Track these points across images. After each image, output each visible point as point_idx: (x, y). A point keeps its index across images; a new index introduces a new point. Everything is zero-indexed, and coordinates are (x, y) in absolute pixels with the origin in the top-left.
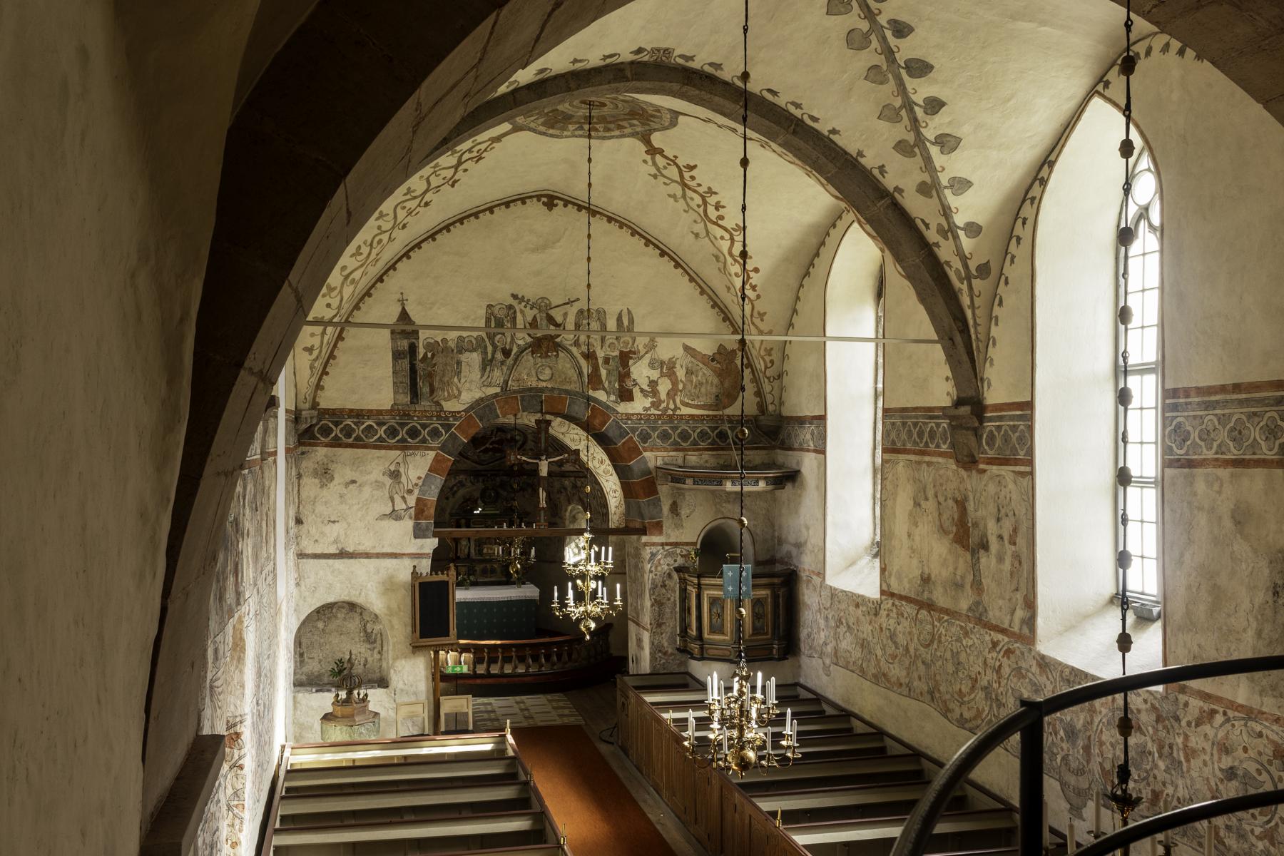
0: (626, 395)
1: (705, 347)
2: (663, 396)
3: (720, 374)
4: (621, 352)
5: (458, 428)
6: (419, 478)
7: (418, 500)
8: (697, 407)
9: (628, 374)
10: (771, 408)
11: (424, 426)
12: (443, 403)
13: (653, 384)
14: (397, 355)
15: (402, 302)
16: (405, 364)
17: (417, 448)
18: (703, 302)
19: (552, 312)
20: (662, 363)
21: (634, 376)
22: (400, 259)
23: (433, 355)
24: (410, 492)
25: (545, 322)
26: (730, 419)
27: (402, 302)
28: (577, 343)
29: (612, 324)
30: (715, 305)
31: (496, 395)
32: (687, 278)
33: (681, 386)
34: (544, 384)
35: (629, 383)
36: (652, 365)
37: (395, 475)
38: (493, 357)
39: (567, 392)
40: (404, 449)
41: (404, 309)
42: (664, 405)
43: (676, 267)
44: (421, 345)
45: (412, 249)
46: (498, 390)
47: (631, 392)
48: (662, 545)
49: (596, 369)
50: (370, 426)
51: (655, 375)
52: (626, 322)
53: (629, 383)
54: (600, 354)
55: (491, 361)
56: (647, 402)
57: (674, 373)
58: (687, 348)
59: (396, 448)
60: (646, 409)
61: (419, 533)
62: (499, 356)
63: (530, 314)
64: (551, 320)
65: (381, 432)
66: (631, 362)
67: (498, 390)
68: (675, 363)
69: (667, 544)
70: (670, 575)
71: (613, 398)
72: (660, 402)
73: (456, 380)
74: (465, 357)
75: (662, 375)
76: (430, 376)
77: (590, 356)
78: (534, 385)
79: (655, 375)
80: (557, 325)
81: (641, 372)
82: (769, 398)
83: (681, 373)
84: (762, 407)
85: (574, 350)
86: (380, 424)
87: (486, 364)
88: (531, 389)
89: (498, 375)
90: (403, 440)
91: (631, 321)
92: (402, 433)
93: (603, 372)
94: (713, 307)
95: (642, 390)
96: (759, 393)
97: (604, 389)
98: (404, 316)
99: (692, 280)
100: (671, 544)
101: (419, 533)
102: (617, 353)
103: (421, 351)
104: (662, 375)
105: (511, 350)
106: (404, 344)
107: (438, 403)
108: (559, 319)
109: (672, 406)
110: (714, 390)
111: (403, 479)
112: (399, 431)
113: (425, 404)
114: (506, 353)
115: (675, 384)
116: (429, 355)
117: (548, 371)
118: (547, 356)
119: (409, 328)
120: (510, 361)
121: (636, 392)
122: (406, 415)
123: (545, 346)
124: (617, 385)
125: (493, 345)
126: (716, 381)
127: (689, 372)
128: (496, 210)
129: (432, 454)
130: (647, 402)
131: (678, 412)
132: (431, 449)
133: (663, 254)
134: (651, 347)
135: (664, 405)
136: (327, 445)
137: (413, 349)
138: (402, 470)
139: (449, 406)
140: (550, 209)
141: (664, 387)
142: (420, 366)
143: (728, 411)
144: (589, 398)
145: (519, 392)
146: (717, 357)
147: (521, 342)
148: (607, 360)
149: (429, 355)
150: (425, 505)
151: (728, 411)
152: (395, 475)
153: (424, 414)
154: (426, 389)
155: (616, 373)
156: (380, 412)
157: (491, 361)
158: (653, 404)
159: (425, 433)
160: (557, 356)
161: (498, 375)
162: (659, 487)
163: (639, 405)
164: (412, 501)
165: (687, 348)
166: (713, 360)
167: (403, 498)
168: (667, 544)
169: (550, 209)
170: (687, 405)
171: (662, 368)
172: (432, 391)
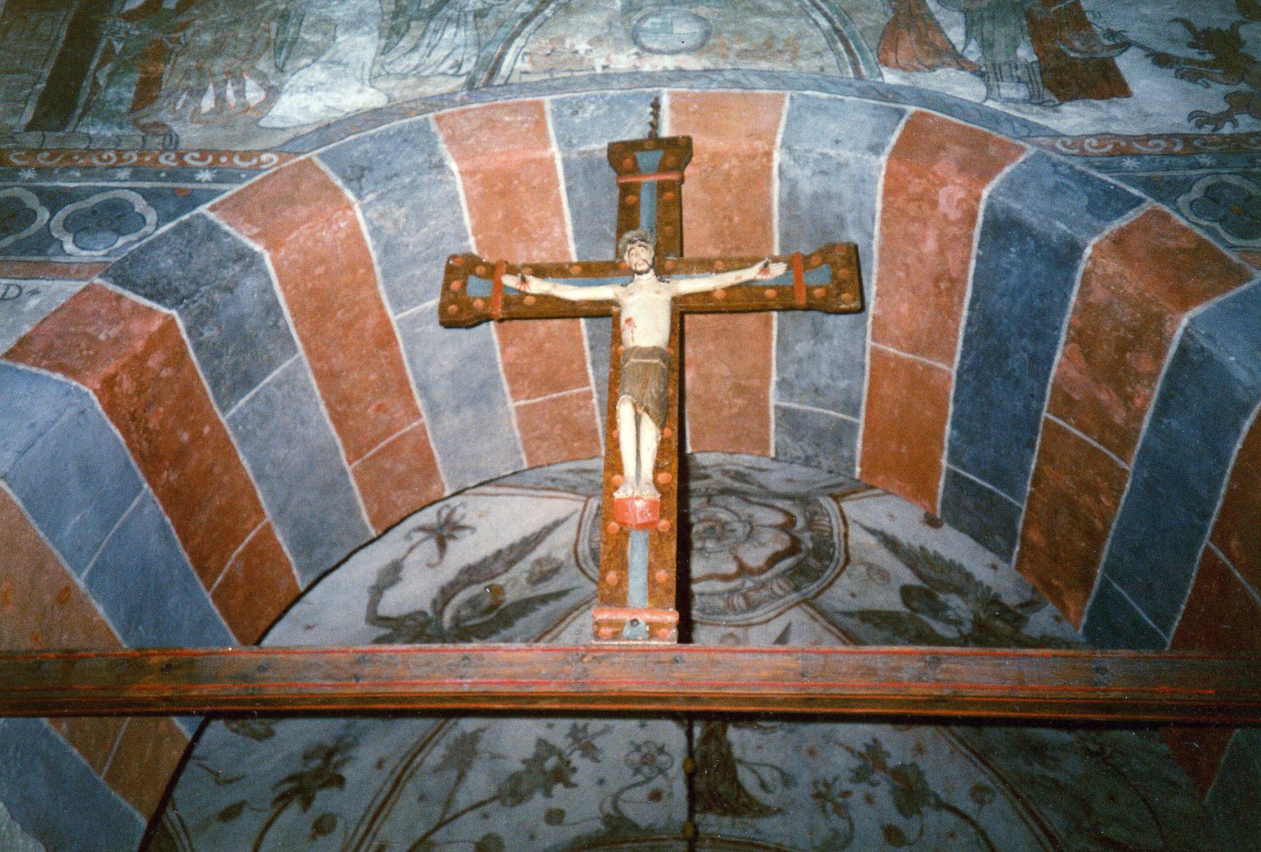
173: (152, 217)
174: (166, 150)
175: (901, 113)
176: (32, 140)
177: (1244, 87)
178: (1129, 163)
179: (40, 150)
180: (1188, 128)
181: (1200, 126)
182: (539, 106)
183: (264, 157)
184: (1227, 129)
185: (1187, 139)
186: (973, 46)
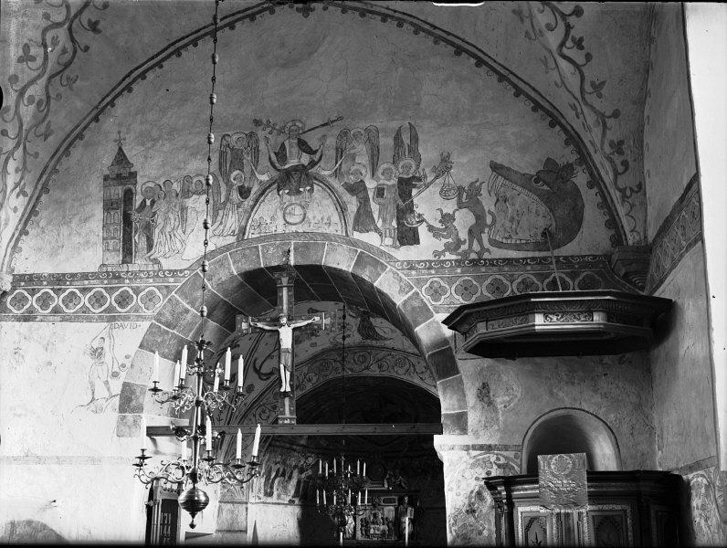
0: (408, 237)
1: (526, 164)
2: (463, 235)
3: (547, 199)
4: (401, 181)
5: (181, 291)
6: (127, 357)
7: (125, 385)
8: (517, 247)
9: (411, 209)
10: (631, 239)
11: (137, 291)
12: (162, 261)
13: (447, 219)
14: (109, 206)
15: (119, 142)
16: (118, 216)
17: (126, 318)
18: (523, 106)
19: (307, 138)
20: (460, 189)
21: (418, 211)
22: (120, 94)
23: (153, 202)
24: (115, 375)
25: (295, 150)
26: (567, 262)
27: (119, 142)
28: (337, 174)
29: (386, 142)
30: (537, 107)
31: (228, 247)
32: (495, 78)
33: (489, 220)
34: (293, 228)
35: (412, 221)
36: (444, 194)
37: (97, 353)
38: (228, 199)
39: (326, 237)
40: (112, 319)
41: (120, 149)
42: (464, 247)
43: (477, 65)
44: (139, 190)
45: (134, 80)
46: (232, 239)
47: (415, 231)
48: (467, 448)
49: (364, 202)
50: (73, 293)
51: (449, 207)
52: (406, 139)
53: (412, 221)
54: (371, 185)
55: (225, 203)
56: (439, 245)
57: (478, 202)
58: (496, 167)
59: (101, 319)
60: (436, 253)
61: (123, 429)
62: (235, 196)
63: (276, 140)
64: (303, 146)
65: (85, 300)
66: (414, 192)
67: (232, 239)
68: (479, 189)
69: (474, 447)
70: (479, 494)
71: (389, 241)
72: (459, 243)
73: (180, 231)
74: (190, 202)
75: (460, 206)
76: (148, 229)
77: (357, 189)
78: (280, 231)
79: (449, 207)
80: (311, 152)
81: (428, 204)
82: (627, 224)
83: (488, 203)
84: (618, 239)
85: (336, 184)
86: (84, 290)
87: (217, 209)
88: (275, 236)
89: (232, 221)
90: (111, 309)
91: (414, 139)
92: (111, 300)
93: (375, 207)
94: (534, 109)
95: (431, 228)
96: (613, 223)
97: (377, 230)
98: (121, 158)
99: (502, 78)
100: (481, 447)
101: (123, 429)
102: (394, 181)
103: (138, 200)
104: (460, 206)
105: (249, 190)
106: (119, 191)
107: (156, 261)
108: (314, 144)
109: (476, 247)
110: (542, 223)
111: (107, 358)
112: (107, 297)
113: (139, 263)
114: (244, 192)
115: (479, 218)
116: (148, 203)
117: (298, 211)
118: (299, 192)
119: (125, 173)
120: (248, 202)
121: (423, 231)
122: (117, 277)
123: (292, 180)
124: (394, 224)
125: (228, 183)
126: (543, 209)
127: (501, 200)
128: (238, 25)
129: (146, 325)
130: (439, 245)
131: (486, 256)
132: (144, 318)
133: (459, 51)
134: (444, 166)
135: (464, 247)
136: (19, 319)
137: (129, 195)
138: (106, 345)
139: (167, 264)
140: (306, 16)
141: (463, 221)
142: (135, 216)
143: (569, 250)
144: (354, 243)
145: (259, 240)
146: (542, 176)
147: (264, 178)
148: (380, 192)
149: (148, 203)
150: (133, 392)
151: (569, 250)
152: (97, 353)
153: (135, 275)
154: (143, 243)
155: (392, 209)
156: (85, 276)
157: (225, 203)
158: (448, 248)
159: (136, 300)
160: (312, 190)
161: (232, 221)
162: (460, 364)
163: (428, 245)
164: (117, 387)
165: (496, 167)
166: (537, 181)
167: (106, 383)
168: (474, 447)
169: (306, 16)
170: (499, 245)
171: (460, 196)
172: (150, 247)
173: (161, 297)
174: (159, 270)
175: (357, 251)
176: (125, 268)
177: (450, 240)
178: (414, 272)
179: (128, 272)
180: (432, 258)
181: (435, 257)
182: (257, 248)
183: (186, 272)
184: (442, 258)
185: (430, 262)
186: (381, 220)
